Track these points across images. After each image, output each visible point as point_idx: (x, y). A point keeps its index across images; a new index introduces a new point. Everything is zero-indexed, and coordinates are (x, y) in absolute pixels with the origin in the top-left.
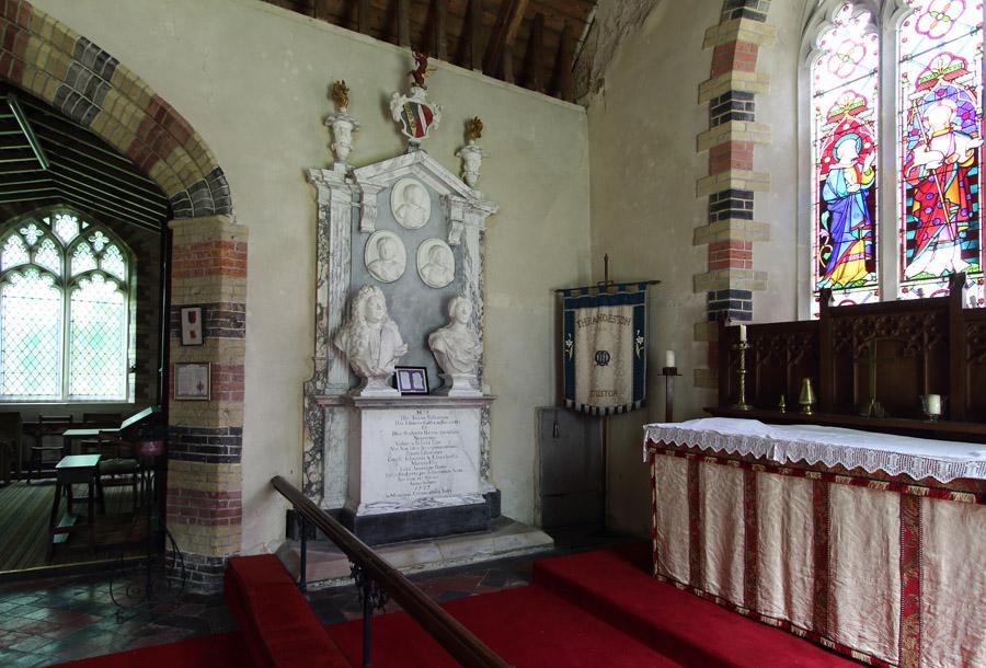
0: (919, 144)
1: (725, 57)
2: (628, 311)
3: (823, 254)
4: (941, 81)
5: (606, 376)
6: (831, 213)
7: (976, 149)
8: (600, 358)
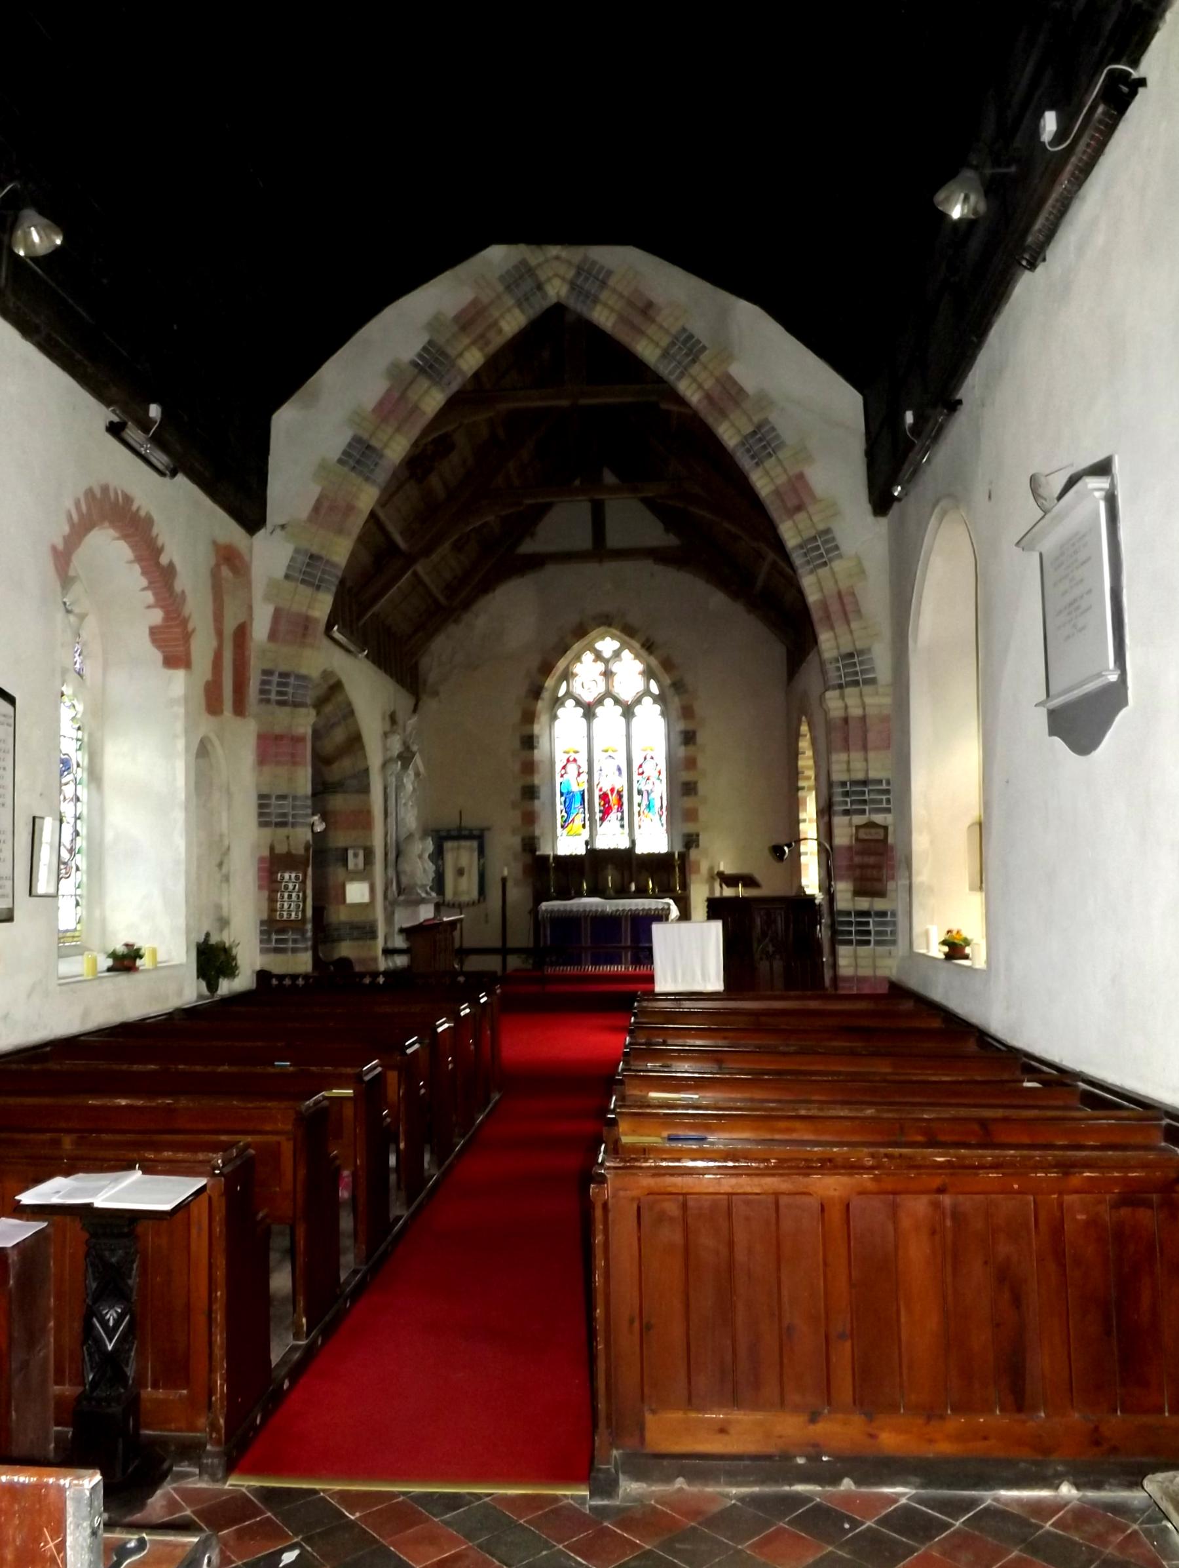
1: (529, 717)
2: (475, 844)
5: (464, 883)
8: (460, 872)
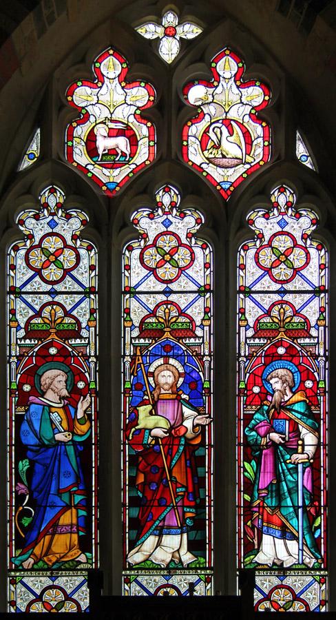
0: (144, 403)
3: (20, 519)
4: (167, 335)
6: (32, 463)
7: (203, 427)
